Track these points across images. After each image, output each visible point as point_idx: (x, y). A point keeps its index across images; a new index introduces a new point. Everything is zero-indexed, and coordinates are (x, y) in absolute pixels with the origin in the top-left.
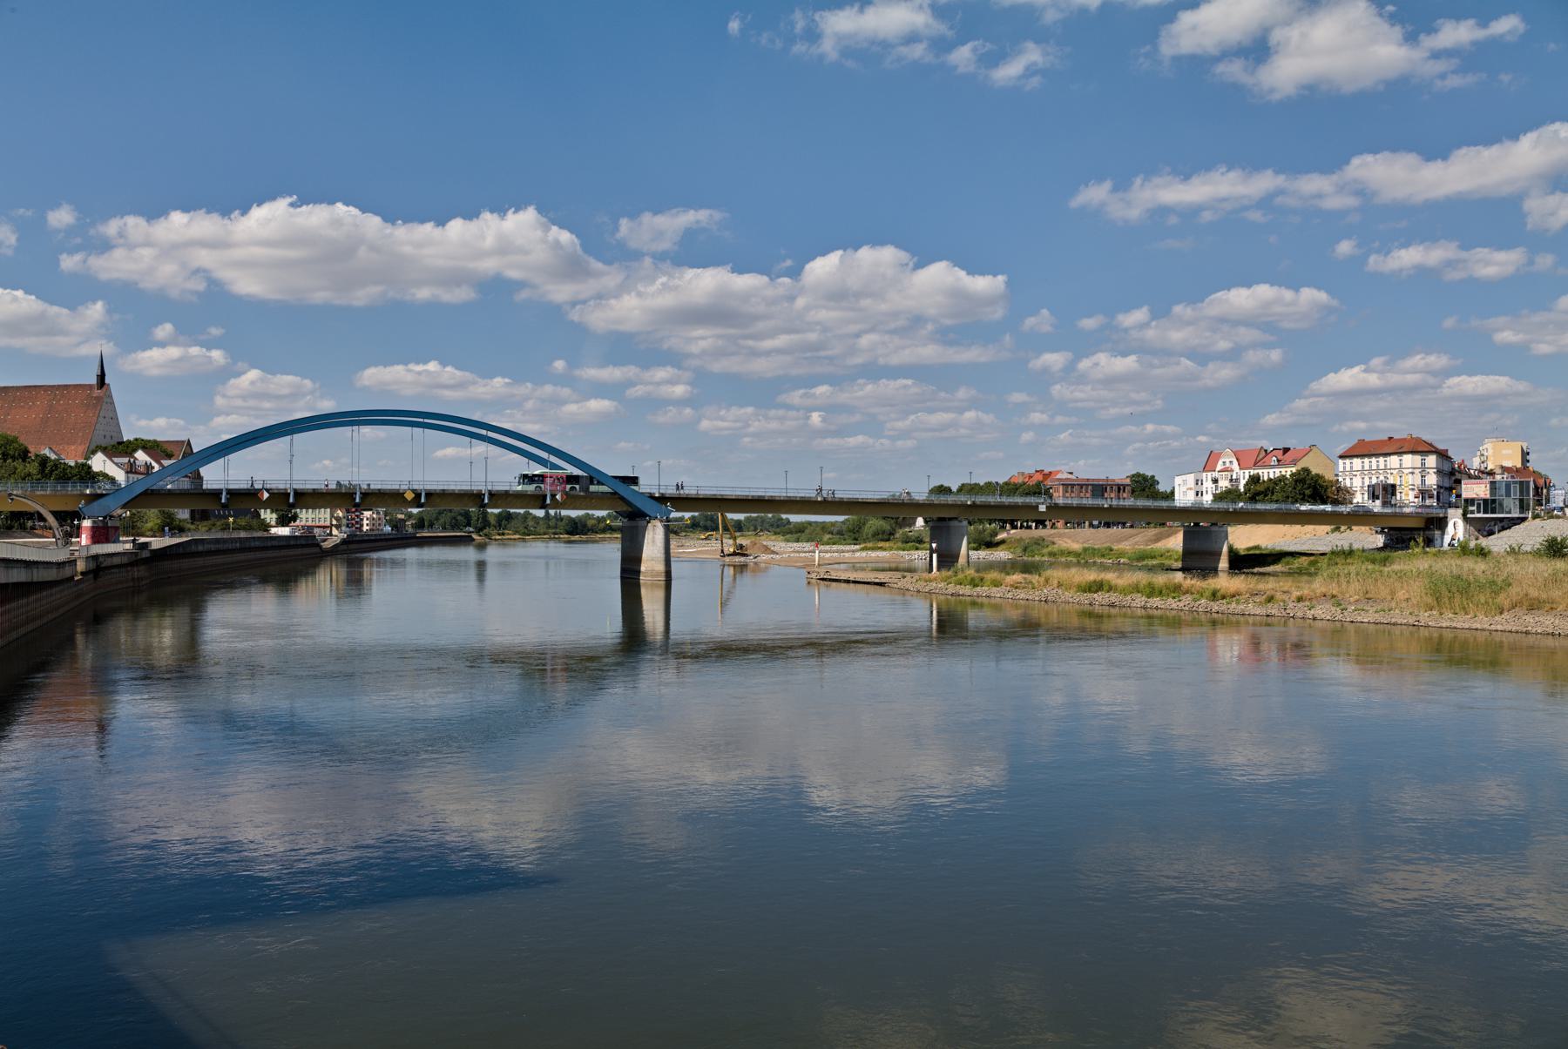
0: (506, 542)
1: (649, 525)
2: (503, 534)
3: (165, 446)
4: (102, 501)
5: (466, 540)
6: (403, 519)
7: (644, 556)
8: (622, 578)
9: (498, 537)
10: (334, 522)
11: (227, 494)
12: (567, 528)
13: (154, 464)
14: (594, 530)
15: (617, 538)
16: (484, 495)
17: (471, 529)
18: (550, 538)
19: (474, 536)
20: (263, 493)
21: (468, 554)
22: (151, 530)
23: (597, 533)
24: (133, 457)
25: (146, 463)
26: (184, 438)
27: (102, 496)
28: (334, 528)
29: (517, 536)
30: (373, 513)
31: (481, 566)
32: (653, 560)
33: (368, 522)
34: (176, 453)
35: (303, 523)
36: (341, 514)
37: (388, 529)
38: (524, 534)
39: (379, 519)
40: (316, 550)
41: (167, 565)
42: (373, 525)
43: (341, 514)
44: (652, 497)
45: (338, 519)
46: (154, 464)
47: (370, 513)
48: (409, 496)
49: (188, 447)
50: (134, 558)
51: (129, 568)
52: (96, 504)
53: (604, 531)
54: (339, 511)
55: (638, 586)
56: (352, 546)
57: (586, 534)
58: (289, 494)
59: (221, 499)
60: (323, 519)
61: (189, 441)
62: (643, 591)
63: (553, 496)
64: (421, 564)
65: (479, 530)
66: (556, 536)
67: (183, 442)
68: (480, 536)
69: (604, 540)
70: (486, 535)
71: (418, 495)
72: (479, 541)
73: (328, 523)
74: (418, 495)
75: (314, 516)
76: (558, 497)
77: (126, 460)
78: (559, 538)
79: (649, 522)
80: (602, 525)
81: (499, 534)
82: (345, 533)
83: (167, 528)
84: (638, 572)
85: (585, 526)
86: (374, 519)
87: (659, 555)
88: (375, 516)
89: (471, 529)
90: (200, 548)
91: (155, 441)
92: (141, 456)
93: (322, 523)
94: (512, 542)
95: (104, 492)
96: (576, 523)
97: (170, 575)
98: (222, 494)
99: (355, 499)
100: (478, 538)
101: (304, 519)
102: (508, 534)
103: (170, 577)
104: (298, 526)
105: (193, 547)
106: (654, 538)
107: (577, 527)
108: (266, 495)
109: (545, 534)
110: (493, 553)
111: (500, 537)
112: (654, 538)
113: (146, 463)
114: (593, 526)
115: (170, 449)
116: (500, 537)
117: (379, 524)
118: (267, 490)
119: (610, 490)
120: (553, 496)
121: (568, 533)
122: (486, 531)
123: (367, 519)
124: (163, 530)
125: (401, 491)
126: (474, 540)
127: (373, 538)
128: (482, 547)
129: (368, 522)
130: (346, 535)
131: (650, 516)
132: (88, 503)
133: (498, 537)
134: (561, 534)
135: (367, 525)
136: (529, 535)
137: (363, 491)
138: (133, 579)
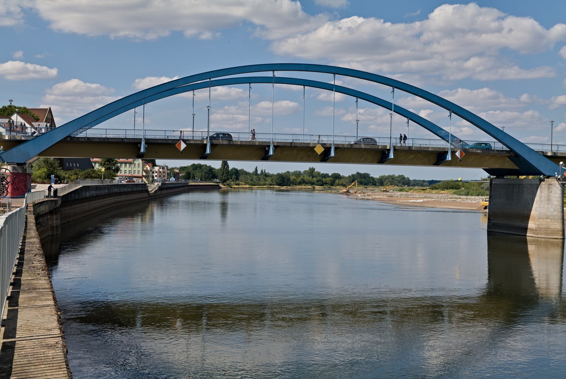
0: (240, 190)
1: (543, 183)
2: (239, 184)
3: (33, 113)
4: (21, 147)
5: (216, 188)
6: (178, 173)
7: (533, 213)
8: (489, 233)
9: (236, 186)
10: (144, 174)
11: (146, 143)
12: (278, 181)
13: (27, 125)
14: (294, 183)
15: (309, 188)
16: (389, 150)
17: (218, 181)
18: (268, 188)
19: (221, 185)
20: (180, 143)
21: (215, 197)
22: (40, 177)
23: (296, 184)
24: (11, 119)
25: (21, 124)
26: (46, 107)
27: (21, 142)
28: (144, 178)
29: (247, 186)
31: (224, 206)
32: (548, 218)
34: (41, 118)
35: (123, 174)
36: (149, 168)
37: (173, 179)
38: (252, 184)
39: (164, 172)
40: (145, 195)
41: (69, 210)
42: (160, 176)
43: (149, 168)
44: (544, 155)
45: (146, 171)
46: (27, 125)
48: (319, 150)
49: (50, 113)
50: (53, 206)
51: (49, 217)
52: (15, 150)
53: (300, 184)
54: (147, 166)
55: (525, 242)
56: (164, 192)
57: (289, 186)
58: (206, 145)
59: (140, 148)
60: (137, 172)
61: (50, 108)
62: (531, 248)
63: (453, 153)
64: (187, 203)
65: (224, 182)
66: (272, 186)
67: (46, 110)
68: (224, 185)
69: (300, 190)
70: (228, 185)
71: (327, 150)
72: (223, 189)
73: (140, 175)
74: (327, 150)
75: (130, 169)
76: (458, 154)
77: (6, 121)
78: (273, 188)
79: (541, 180)
80: (299, 180)
81: (236, 185)
82: (159, 182)
83: (53, 176)
84: (526, 229)
85: (289, 179)
86: (160, 172)
87: (555, 213)
88: (161, 170)
89: (218, 181)
90: (88, 194)
91: (25, 108)
92: (16, 119)
93: (136, 174)
94: (242, 190)
95: (23, 139)
96: (284, 178)
97: (70, 220)
98: (141, 143)
99: (268, 152)
100: (224, 186)
101: (123, 172)
102: (242, 184)
103: (69, 222)
104: (123, 176)
105: (84, 193)
106: (549, 196)
107: (284, 181)
108: (183, 146)
109: (264, 185)
110: (231, 198)
111: (237, 186)
112: (549, 196)
113: (21, 124)
114: (294, 180)
115: (36, 114)
117: (164, 176)
118: (185, 141)
119: (505, 148)
120: (453, 153)
121: (277, 185)
122: (228, 182)
124: (50, 178)
125: (311, 145)
126: (220, 188)
127: (172, 186)
128: (225, 193)
129: (156, 174)
130: (160, 184)
131: (544, 175)
132: (5, 149)
133: (236, 186)
134: (274, 185)
136: (255, 185)
137: (276, 144)
138: (52, 228)
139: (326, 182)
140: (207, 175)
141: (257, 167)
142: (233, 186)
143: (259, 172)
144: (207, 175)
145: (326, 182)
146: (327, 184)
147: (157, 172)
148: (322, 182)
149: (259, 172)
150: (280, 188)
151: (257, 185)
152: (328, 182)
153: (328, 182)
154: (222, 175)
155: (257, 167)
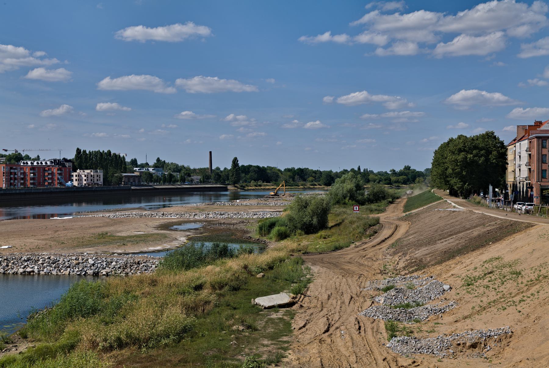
2: (260, 186)
19: (229, 187)
30: (91, 171)
33: (85, 178)
42: (91, 180)
47: (89, 171)
66: (312, 187)
68: (236, 187)
81: (256, 186)
86: (91, 176)
88: (92, 173)
100: (233, 188)
116: (254, 188)
123: (85, 176)
129: (85, 178)
135: (85, 180)
139: (398, 180)
140: (217, 176)
141: (359, 166)
142: (246, 188)
143: (362, 171)
144: (217, 176)
145: (398, 180)
146: (399, 182)
147: (86, 176)
148: (390, 180)
149: (362, 171)
150: (323, 188)
151: (289, 186)
152: (400, 180)
153: (400, 180)
154: (232, 176)
155: (359, 166)
